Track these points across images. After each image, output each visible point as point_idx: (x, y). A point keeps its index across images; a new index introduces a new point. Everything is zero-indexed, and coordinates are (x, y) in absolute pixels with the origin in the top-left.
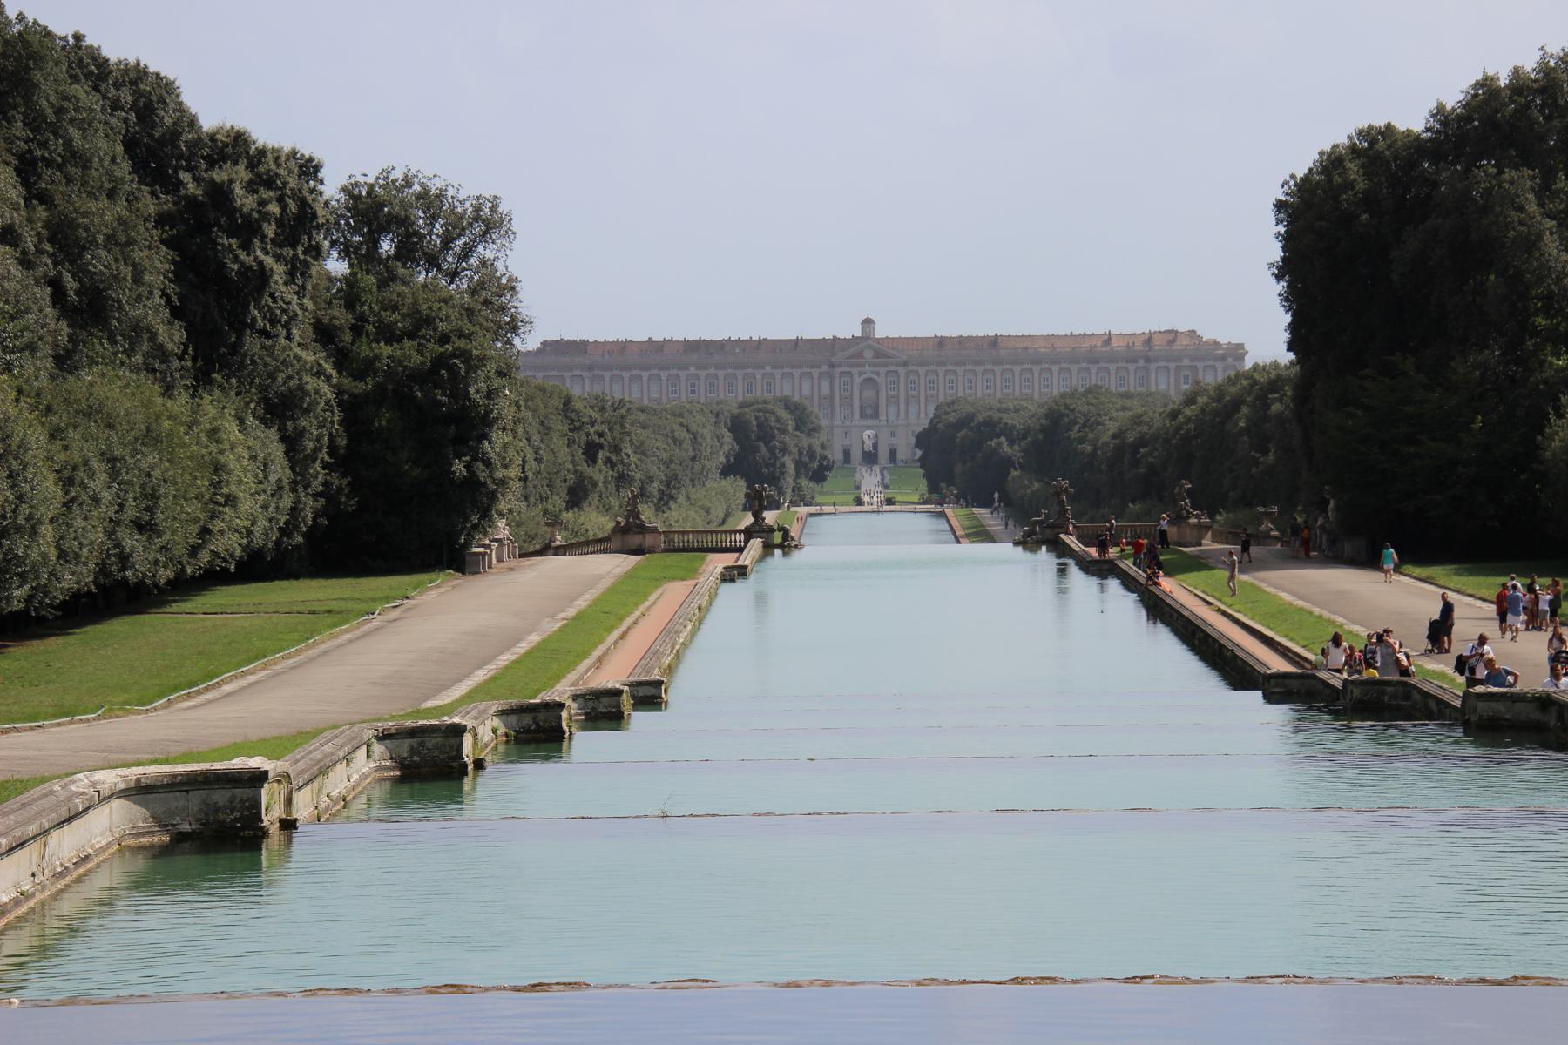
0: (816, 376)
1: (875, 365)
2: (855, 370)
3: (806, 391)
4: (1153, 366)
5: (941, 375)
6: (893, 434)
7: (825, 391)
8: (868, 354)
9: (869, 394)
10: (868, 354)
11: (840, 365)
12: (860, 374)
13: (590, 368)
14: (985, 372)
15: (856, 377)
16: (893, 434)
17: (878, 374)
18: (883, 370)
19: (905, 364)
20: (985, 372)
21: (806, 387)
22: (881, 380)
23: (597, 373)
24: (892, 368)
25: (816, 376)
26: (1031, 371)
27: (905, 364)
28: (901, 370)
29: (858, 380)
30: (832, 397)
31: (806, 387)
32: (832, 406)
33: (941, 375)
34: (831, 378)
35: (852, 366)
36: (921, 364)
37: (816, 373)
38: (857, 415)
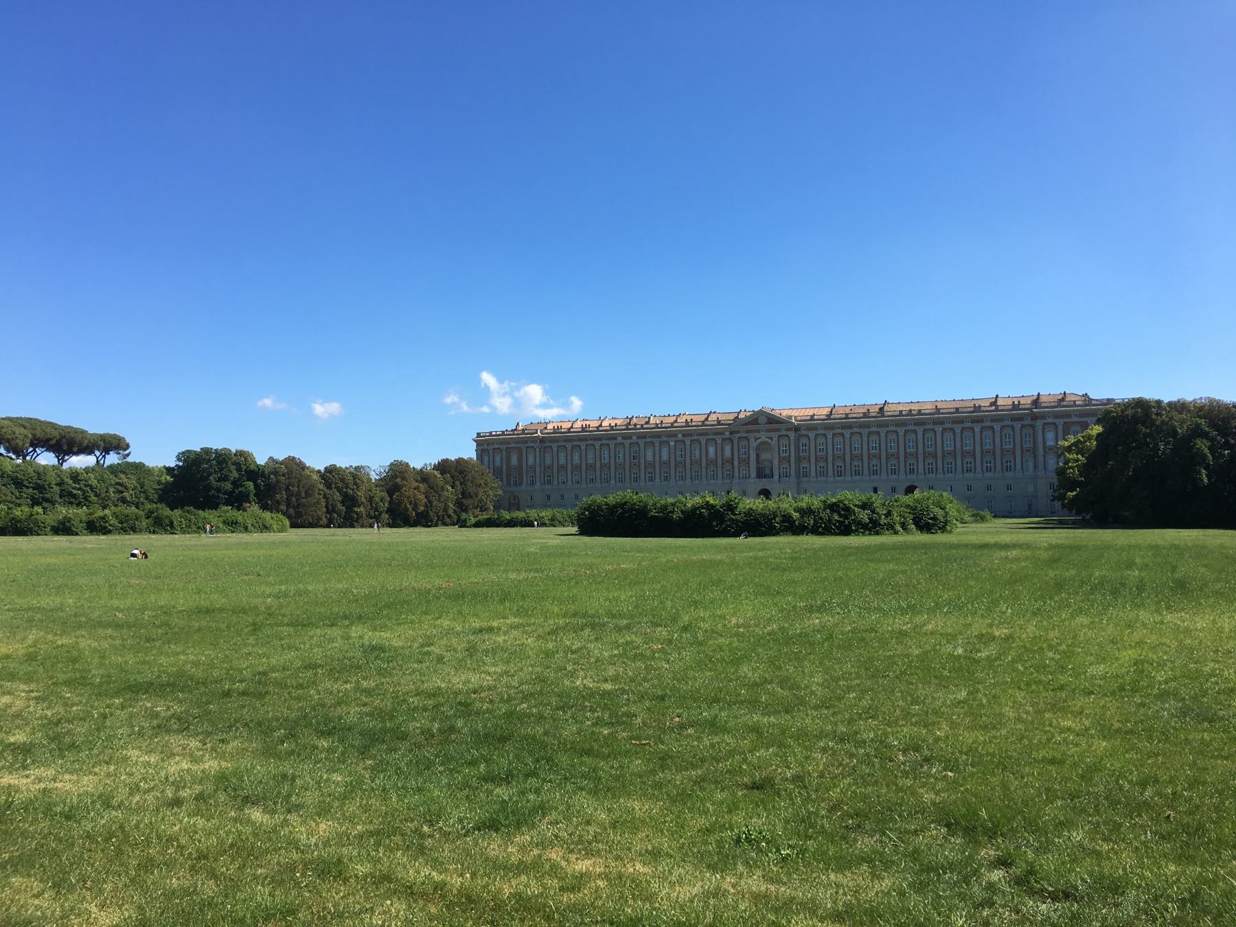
0: (719, 442)
1: (768, 431)
2: (751, 436)
4: (1039, 424)
7: (728, 453)
8: (762, 420)
10: (762, 420)
12: (756, 439)
17: (771, 438)
18: (775, 435)
21: (711, 450)
22: (774, 443)
25: (719, 442)
29: (754, 444)
31: (711, 450)
35: (748, 432)
38: (753, 474)
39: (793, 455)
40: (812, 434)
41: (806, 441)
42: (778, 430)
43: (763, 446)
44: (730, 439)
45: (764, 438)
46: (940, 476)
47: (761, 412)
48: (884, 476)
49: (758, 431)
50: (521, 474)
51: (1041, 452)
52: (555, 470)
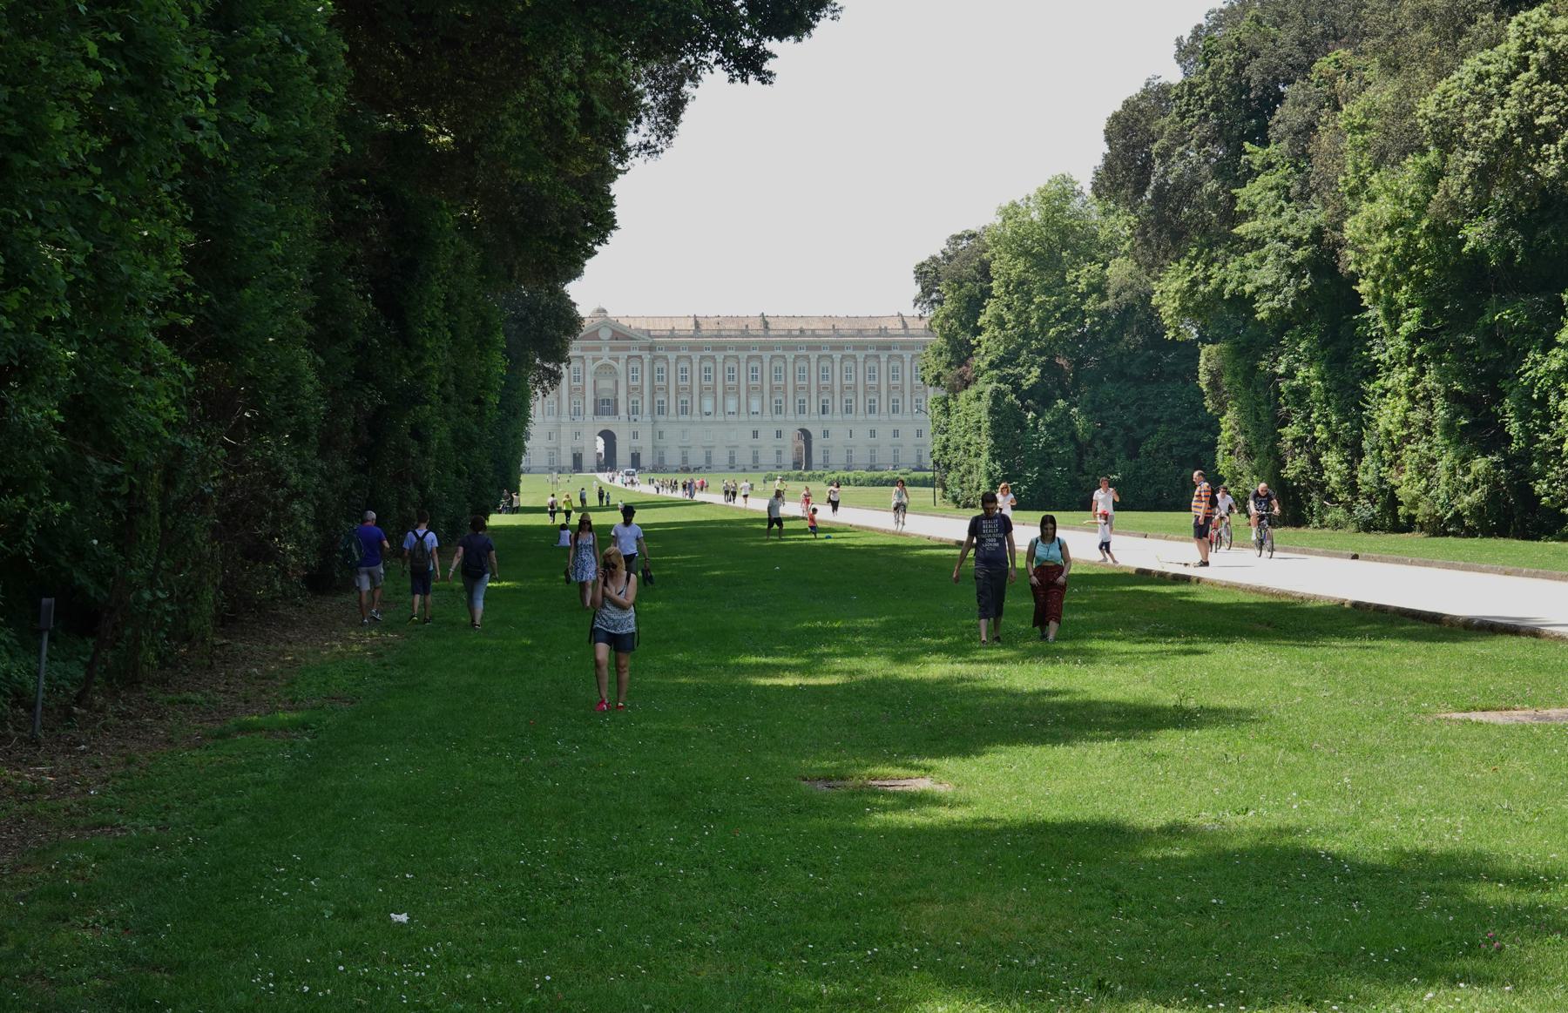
1: (612, 349)
2: (589, 355)
5: (696, 361)
6: (635, 435)
8: (605, 334)
12: (595, 360)
14: (750, 358)
15: (589, 362)
16: (635, 435)
17: (617, 359)
18: (623, 355)
19: (651, 348)
20: (750, 358)
22: (620, 367)
24: (636, 353)
26: (807, 358)
27: (651, 348)
28: (646, 356)
29: (591, 367)
33: (696, 361)
36: (670, 348)
38: (590, 408)
40: (672, 356)
41: (664, 365)
42: (628, 349)
43: (607, 370)
45: (606, 360)
46: (838, 417)
48: (767, 417)
49: (599, 349)
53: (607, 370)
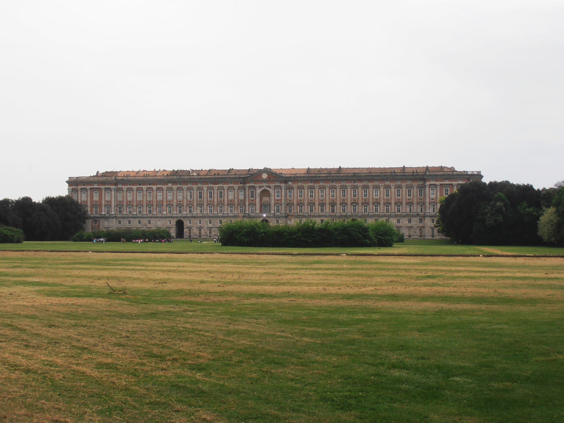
2: (257, 185)
3: (231, 197)
7: (241, 197)
8: (265, 176)
9: (265, 199)
10: (265, 176)
11: (249, 183)
12: (260, 187)
13: (116, 184)
17: (270, 187)
18: (272, 185)
22: (271, 191)
23: (120, 186)
27: (286, 182)
28: (283, 185)
29: (259, 191)
30: (245, 200)
32: (245, 205)
34: (245, 189)
35: (256, 182)
37: (236, 186)
39: (283, 198)
44: (243, 187)
47: (266, 170)
50: (100, 206)
51: (428, 201)
52: (125, 204)
53: (265, 193)
